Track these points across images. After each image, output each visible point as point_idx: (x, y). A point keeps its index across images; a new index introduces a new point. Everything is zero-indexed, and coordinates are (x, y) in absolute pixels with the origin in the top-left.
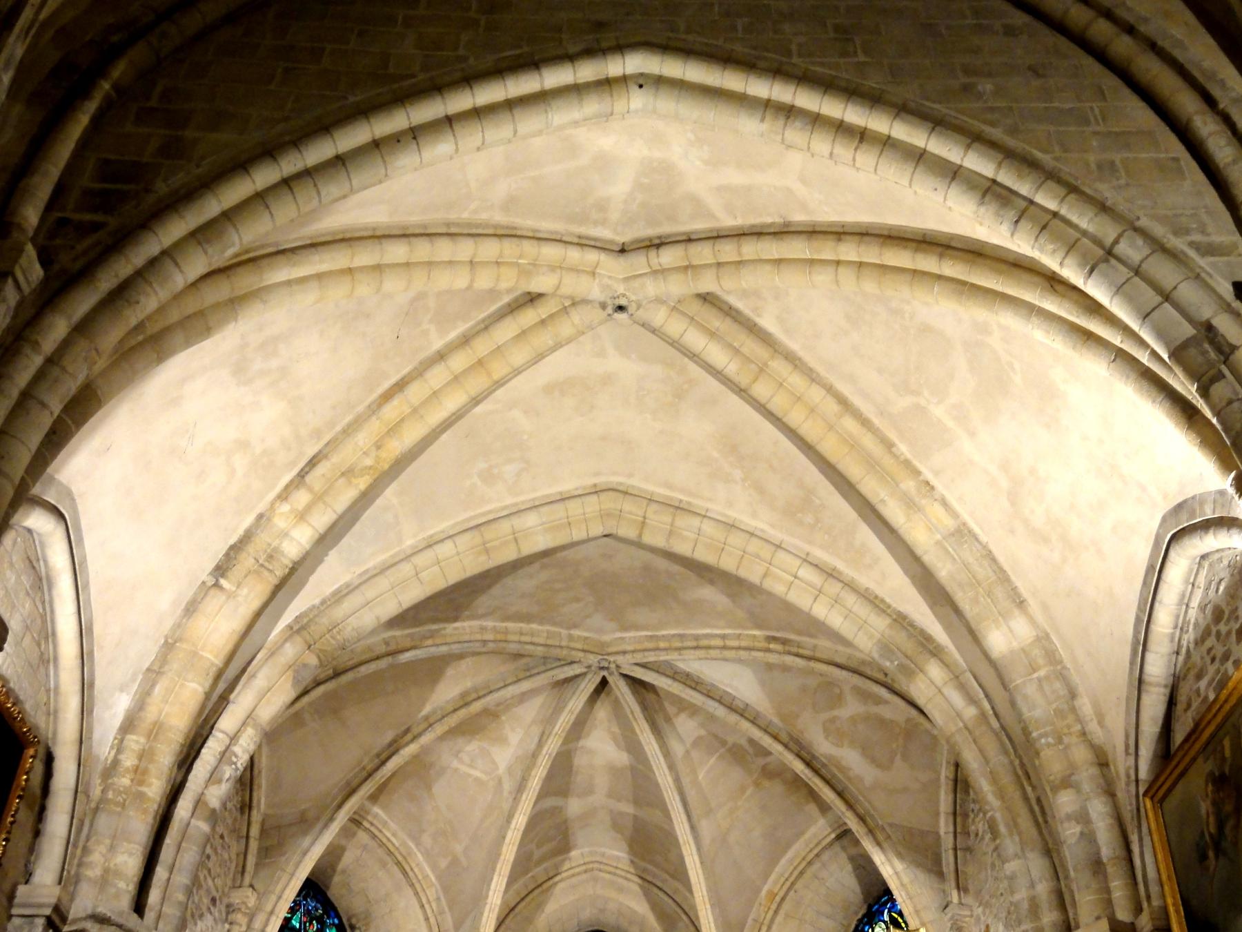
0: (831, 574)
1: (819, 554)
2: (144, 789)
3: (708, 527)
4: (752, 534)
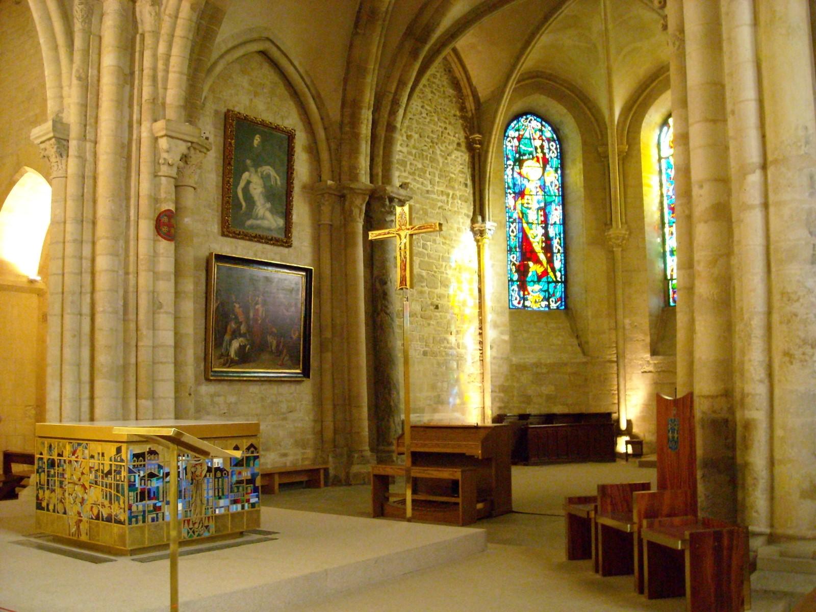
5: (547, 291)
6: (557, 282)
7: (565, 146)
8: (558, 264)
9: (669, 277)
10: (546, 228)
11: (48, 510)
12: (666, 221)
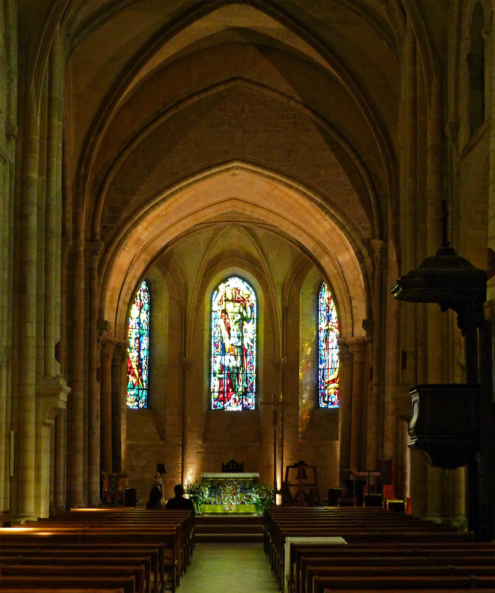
0: (300, 228)
1: (296, 221)
2: (113, 305)
3: (263, 212)
4: (277, 214)
5: (138, 395)
6: (143, 389)
7: (154, 297)
8: (145, 378)
9: (212, 391)
10: (139, 352)
11: (210, 503)
12: (213, 353)
